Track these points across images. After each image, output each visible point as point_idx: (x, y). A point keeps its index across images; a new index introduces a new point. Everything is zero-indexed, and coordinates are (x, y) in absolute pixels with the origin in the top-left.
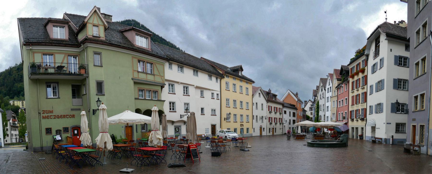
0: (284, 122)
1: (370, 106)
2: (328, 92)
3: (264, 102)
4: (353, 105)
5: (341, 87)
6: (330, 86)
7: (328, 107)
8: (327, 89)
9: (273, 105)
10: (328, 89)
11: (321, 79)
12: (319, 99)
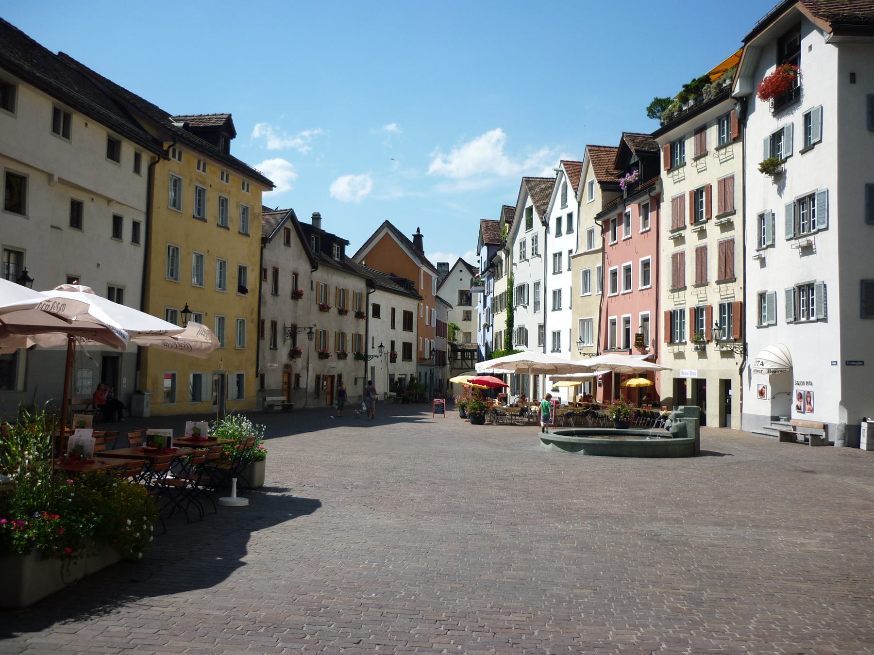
0: (371, 352)
1: (762, 296)
2: (559, 233)
3: (304, 267)
4: (678, 286)
8: (553, 224)
10: (559, 220)
12: (516, 258)
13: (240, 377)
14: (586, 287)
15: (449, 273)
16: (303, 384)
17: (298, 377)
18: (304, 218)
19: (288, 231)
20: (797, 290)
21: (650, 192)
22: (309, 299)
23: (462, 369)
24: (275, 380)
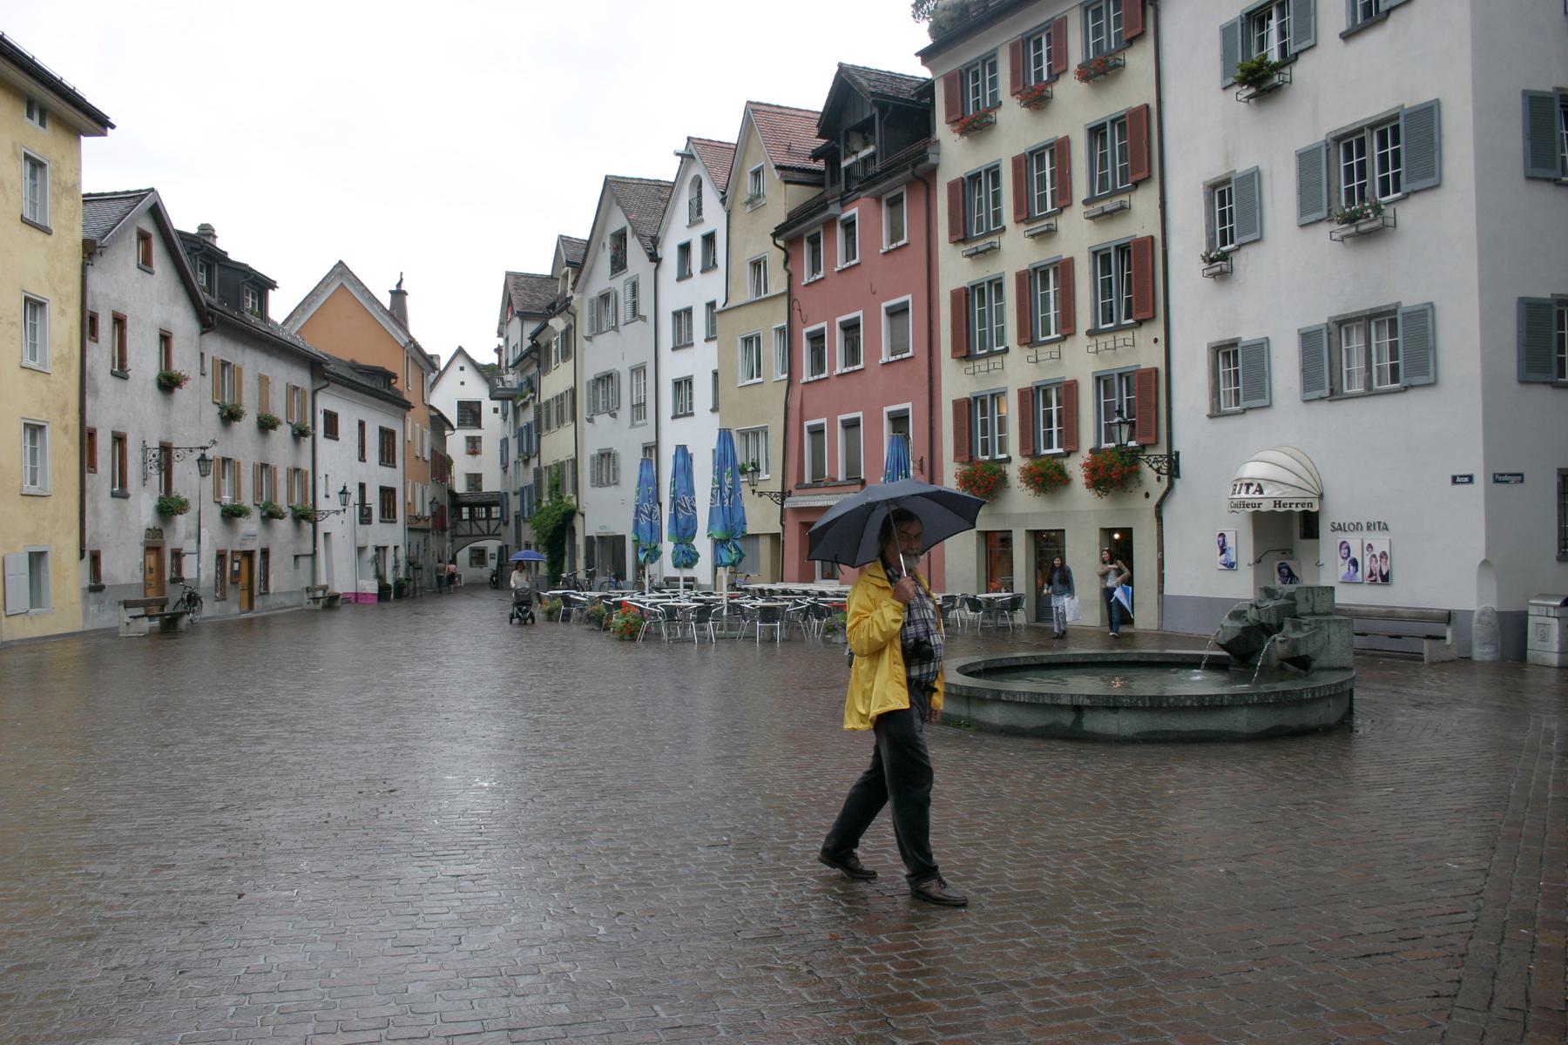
0: (322, 505)
2: (684, 274)
3: (183, 322)
5: (830, 224)
6: (705, 229)
7: (683, 385)
8: (669, 254)
9: (251, 363)
10: (685, 249)
11: (615, 190)
13: (36, 559)
14: (756, 369)
15: (441, 374)
16: (189, 571)
17: (177, 555)
18: (184, 220)
19: (144, 237)
20: (1334, 327)
21: (914, 166)
22: (196, 398)
23: (471, 535)
24: (125, 565)
